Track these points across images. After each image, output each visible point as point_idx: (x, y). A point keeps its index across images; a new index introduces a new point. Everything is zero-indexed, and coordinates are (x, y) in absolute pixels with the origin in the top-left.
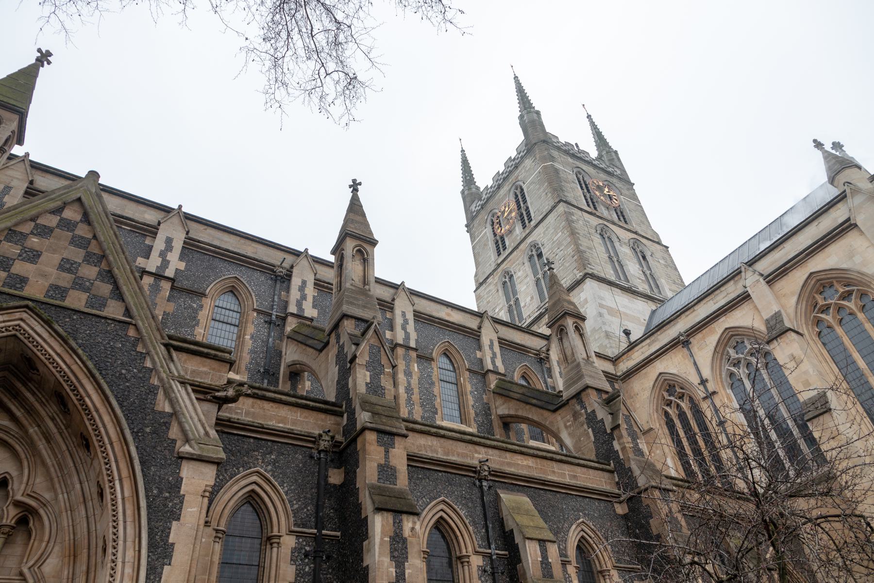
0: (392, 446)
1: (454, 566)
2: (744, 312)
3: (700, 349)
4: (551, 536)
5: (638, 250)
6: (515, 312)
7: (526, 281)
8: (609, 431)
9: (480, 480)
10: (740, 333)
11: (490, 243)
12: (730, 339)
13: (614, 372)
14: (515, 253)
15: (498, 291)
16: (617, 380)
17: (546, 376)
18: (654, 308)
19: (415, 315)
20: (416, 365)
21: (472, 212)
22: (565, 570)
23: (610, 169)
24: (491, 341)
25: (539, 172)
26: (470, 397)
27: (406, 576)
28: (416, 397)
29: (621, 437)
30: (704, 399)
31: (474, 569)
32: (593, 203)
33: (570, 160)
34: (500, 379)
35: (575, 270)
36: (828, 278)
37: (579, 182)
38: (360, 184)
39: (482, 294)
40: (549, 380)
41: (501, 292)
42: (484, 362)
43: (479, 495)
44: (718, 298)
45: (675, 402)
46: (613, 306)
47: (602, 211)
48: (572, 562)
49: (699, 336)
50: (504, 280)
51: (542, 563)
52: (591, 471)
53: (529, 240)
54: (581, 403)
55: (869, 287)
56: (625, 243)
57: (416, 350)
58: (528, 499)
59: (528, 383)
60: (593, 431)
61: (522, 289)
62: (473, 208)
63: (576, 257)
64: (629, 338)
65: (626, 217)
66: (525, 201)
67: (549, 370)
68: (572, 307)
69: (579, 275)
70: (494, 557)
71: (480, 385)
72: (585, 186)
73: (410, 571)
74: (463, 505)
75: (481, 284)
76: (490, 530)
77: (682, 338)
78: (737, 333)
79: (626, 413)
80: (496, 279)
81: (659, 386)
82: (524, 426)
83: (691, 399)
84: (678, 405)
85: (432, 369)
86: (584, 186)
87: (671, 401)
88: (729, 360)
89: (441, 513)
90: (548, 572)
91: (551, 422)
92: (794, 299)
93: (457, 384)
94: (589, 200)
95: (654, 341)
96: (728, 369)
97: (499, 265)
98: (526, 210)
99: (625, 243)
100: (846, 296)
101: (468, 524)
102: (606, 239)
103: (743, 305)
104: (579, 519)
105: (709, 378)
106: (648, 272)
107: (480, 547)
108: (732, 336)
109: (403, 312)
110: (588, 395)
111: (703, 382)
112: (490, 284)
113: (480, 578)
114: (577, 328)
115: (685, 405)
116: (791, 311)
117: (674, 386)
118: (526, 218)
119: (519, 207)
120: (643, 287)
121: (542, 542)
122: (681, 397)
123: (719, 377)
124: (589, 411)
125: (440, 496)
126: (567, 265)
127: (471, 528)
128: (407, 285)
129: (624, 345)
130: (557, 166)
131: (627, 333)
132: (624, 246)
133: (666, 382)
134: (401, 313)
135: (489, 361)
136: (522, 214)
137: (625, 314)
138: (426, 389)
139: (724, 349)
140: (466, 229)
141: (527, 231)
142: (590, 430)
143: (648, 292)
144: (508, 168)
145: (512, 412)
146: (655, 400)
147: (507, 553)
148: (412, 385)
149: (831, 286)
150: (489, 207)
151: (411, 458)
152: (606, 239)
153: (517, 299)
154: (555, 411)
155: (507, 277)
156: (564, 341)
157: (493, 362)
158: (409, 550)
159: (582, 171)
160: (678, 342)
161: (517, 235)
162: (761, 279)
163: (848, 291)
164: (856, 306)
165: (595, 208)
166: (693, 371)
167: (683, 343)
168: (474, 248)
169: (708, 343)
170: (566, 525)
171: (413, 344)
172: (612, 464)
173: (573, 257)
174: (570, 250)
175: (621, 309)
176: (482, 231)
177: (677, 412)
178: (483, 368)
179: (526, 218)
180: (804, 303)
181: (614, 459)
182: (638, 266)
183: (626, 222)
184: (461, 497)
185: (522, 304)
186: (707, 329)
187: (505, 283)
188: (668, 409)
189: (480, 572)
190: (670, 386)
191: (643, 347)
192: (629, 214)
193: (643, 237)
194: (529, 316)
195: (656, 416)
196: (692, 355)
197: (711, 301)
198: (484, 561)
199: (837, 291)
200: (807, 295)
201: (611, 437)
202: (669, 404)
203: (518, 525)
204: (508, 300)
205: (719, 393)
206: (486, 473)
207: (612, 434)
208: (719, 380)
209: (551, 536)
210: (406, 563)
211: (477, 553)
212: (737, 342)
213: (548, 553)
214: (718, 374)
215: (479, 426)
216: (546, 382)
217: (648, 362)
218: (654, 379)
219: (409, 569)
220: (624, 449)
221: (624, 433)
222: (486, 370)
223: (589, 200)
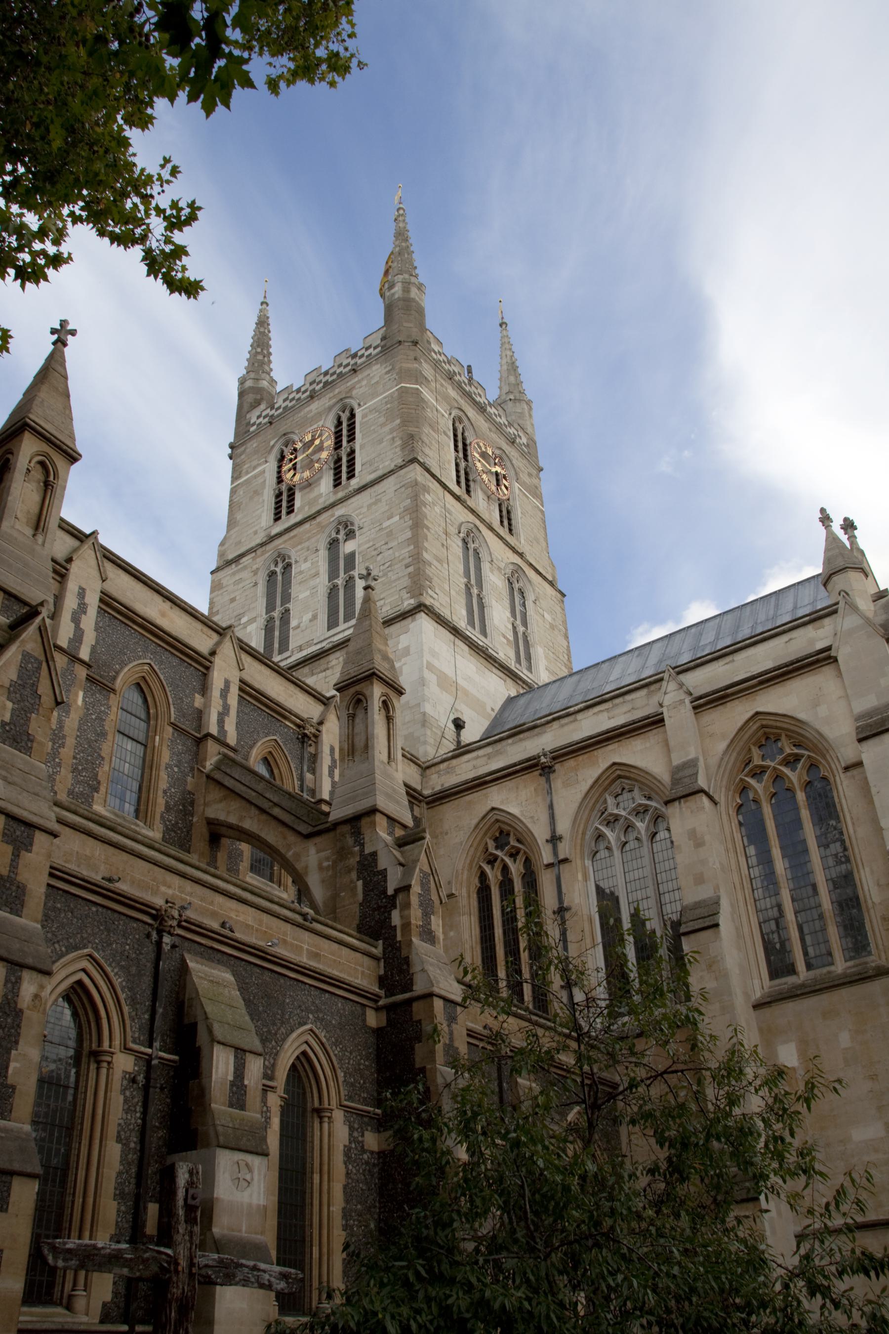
0: (28, 846)
1: (84, 1066)
2: (648, 745)
4: (258, 1046)
6: (277, 633)
7: (312, 583)
8: (390, 892)
9: (160, 932)
10: (632, 776)
11: (266, 492)
13: (419, 788)
14: (307, 526)
15: (256, 584)
16: (420, 801)
17: (305, 768)
18: (513, 693)
19: (101, 600)
20: (81, 694)
21: (249, 424)
22: (264, 1101)
23: (511, 430)
24: (227, 683)
25: (391, 395)
26: (163, 775)
27: (10, 1071)
28: (67, 752)
29: (407, 905)
30: (549, 866)
31: (117, 1075)
32: (467, 480)
33: (452, 393)
34: (225, 756)
36: (777, 728)
37: (455, 436)
38: (73, 333)
39: (224, 582)
40: (309, 776)
41: (261, 589)
42: (205, 717)
43: (152, 956)
44: (617, 711)
45: (503, 860)
46: (449, 671)
47: (479, 500)
48: (278, 1089)
49: (571, 763)
50: (273, 568)
51: (233, 1084)
52: (345, 951)
53: (339, 511)
54: (357, 834)
55: (824, 757)
56: (499, 569)
57: (88, 665)
58: (232, 979)
59: (272, 772)
60: (365, 885)
61: (301, 596)
62: (253, 417)
63: (411, 569)
64: (458, 735)
65: (513, 522)
66: (352, 438)
67: (314, 758)
68: (387, 666)
69: (409, 603)
70: (155, 1062)
71: (187, 757)
72: (462, 447)
73: (18, 1065)
74: (122, 967)
75: (229, 563)
76: (157, 1017)
77: (543, 760)
78: (628, 774)
79: (426, 868)
80: (261, 563)
81: (484, 829)
82: (245, 848)
83: (527, 862)
84: (505, 869)
85: (109, 707)
86: (460, 445)
87: (496, 858)
88: (603, 813)
89: (82, 976)
90: (238, 1099)
91: (297, 856)
92: (722, 745)
94: (462, 473)
95: (498, 753)
96: (597, 828)
97: (272, 539)
98: (349, 455)
99: (499, 569)
100: (792, 761)
101: (123, 1002)
102: (471, 552)
103: (650, 734)
104: (305, 1024)
105: (564, 835)
106: (521, 629)
107: (134, 1042)
108: (619, 777)
109: (81, 588)
110: (373, 824)
111: (554, 839)
112: (245, 568)
113: (123, 1092)
114: (386, 705)
115: (516, 869)
116: (714, 761)
117: (508, 834)
118: (344, 469)
119: (338, 445)
120: (505, 653)
121: (240, 1052)
122: (513, 855)
123: (580, 836)
124: (367, 852)
125: (85, 947)
126: (393, 578)
127: (126, 1009)
128: (103, 540)
129: (449, 746)
130: (426, 394)
131: (459, 725)
132: (496, 572)
133: (497, 825)
134: (77, 589)
135: (214, 718)
136: (339, 460)
137: (466, 693)
138: (89, 742)
139: (600, 796)
140: (229, 451)
141: (340, 495)
142: (360, 883)
143: (513, 665)
144: (340, 365)
145: (233, 820)
146: (473, 849)
147: (176, 1058)
148: (66, 728)
150: (283, 427)
151: (55, 873)
152: (471, 552)
153: (287, 611)
154: (308, 836)
155: (280, 565)
156: (357, 720)
157: (221, 722)
158: (24, 1030)
159: (464, 418)
161: (321, 495)
162: (687, 700)
163: (796, 755)
164: (799, 780)
165: (468, 492)
166: (544, 817)
167: (543, 769)
168: (233, 492)
169: (580, 778)
170: (283, 1030)
171: (84, 654)
172: (380, 948)
173: (407, 566)
174: (405, 551)
175: (460, 681)
176: (259, 465)
177: (500, 878)
178: (199, 727)
179: (344, 469)
180: (735, 754)
181: (385, 940)
182: (508, 614)
183: (510, 530)
184: (122, 953)
185: (293, 623)
186: (586, 756)
187: (273, 574)
188: (487, 869)
189: (125, 1082)
190: (501, 832)
191: (478, 757)
193: (531, 565)
194: (301, 648)
195: (465, 877)
196: (550, 792)
197: (605, 714)
198: (135, 1065)
199: (781, 750)
200: (741, 743)
201: (391, 902)
202: (492, 860)
203: (207, 1018)
204: (270, 607)
205: (573, 863)
206: (175, 923)
207: (394, 896)
208: (579, 841)
209: (257, 1045)
210: (13, 1052)
211: (126, 1049)
213: (246, 1070)
214: (580, 832)
215: (167, 831)
216: (302, 779)
218: (481, 815)
219: (17, 1061)
220: (407, 926)
221: (414, 900)
222: (204, 732)
223: (462, 473)
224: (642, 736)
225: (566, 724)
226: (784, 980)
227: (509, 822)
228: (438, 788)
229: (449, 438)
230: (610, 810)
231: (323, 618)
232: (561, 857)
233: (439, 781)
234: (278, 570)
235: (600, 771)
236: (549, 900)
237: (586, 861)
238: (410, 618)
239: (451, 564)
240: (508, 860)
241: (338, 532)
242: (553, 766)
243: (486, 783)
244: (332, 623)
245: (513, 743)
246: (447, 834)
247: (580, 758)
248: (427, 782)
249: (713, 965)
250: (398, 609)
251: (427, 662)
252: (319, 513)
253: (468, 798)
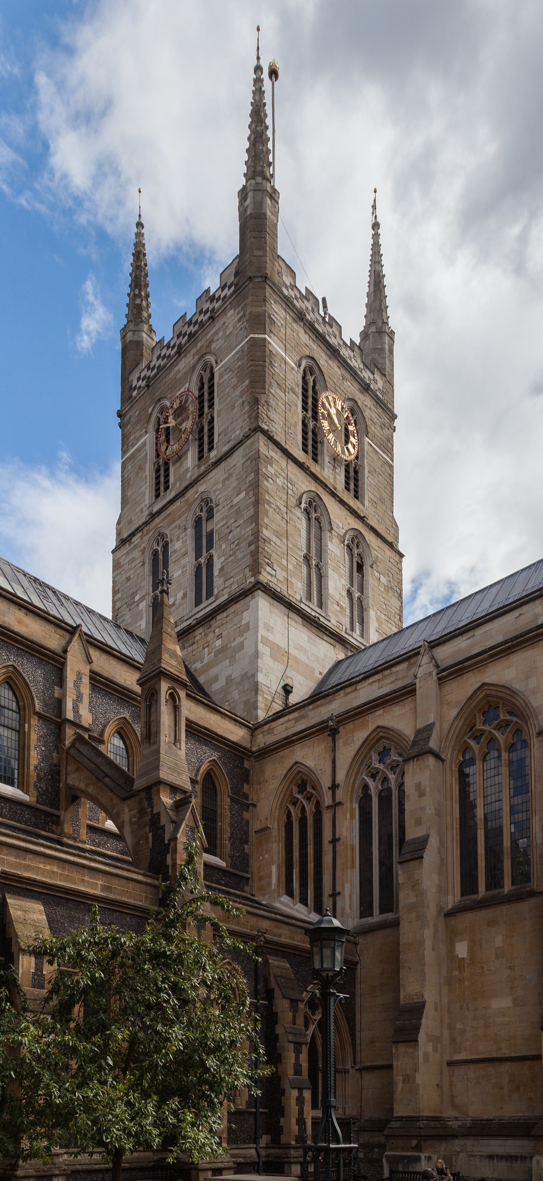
3: (346, 744)
5: (356, 552)
12: (378, 740)
16: (249, 756)
30: (329, 807)
35: (247, 570)
36: (497, 697)
49: (350, 726)
77: (331, 723)
78: (387, 735)
81: (291, 778)
83: (318, 804)
84: (303, 808)
88: (369, 767)
93: (19, 732)
95: (302, 717)
103: (406, 701)
108: (382, 737)
111: (334, 787)
115: (309, 809)
116: (446, 726)
122: (309, 799)
123: (351, 785)
126: (240, 556)
129: (278, 707)
137: (297, 660)
139: (368, 752)
149: (497, 708)
160: (327, 727)
163: (507, 721)
164: (506, 741)
166: (329, 770)
167: (330, 730)
169: (355, 739)
186: (361, 720)
190: (303, 780)
191: (289, 721)
192: (368, 480)
196: (334, 750)
199: (498, 716)
200: (469, 710)
208: (350, 789)
212: (385, 747)
214: (352, 782)
217: (288, 742)
218: (289, 767)
224: (401, 703)
225: (350, 693)
226: (469, 897)
227: (307, 773)
228: (262, 745)
230: (373, 765)
232: (337, 801)
233: (263, 740)
235: (368, 732)
236: (327, 834)
237: (354, 804)
238: (250, 596)
240: (305, 803)
241: (201, 511)
242: (338, 728)
243: (293, 741)
245: (313, 709)
246: (267, 781)
247: (357, 722)
248: (255, 741)
249: (415, 885)
250: (242, 586)
251: (262, 635)
253: (281, 754)
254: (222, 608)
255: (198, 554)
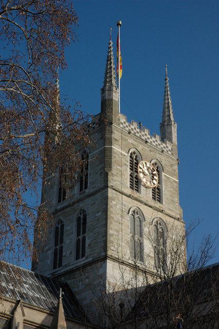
33: (131, 141)
35: (102, 248)
53: (81, 205)
72: (134, 166)
126: (99, 241)
141: (82, 196)
185: (64, 254)
204: (56, 245)
229: (127, 166)
231: (74, 253)
234: (59, 226)
239: (123, 231)
241: (81, 214)
244: (77, 258)
252: (74, 203)
254: (90, 264)
255: (78, 234)
